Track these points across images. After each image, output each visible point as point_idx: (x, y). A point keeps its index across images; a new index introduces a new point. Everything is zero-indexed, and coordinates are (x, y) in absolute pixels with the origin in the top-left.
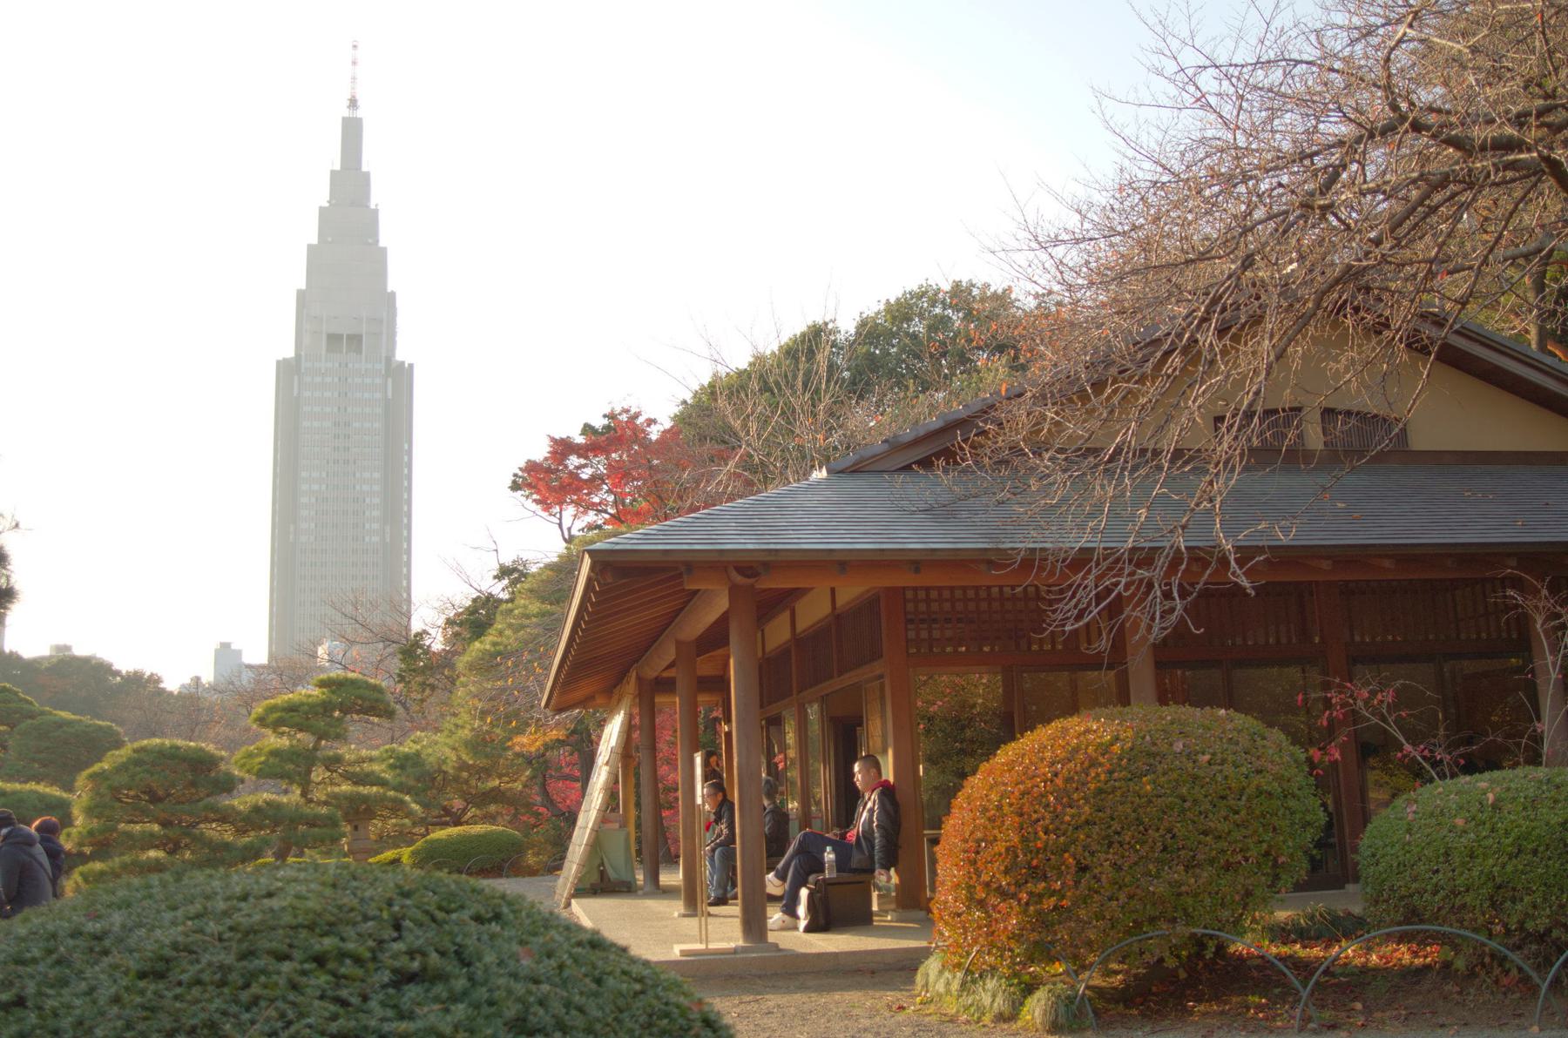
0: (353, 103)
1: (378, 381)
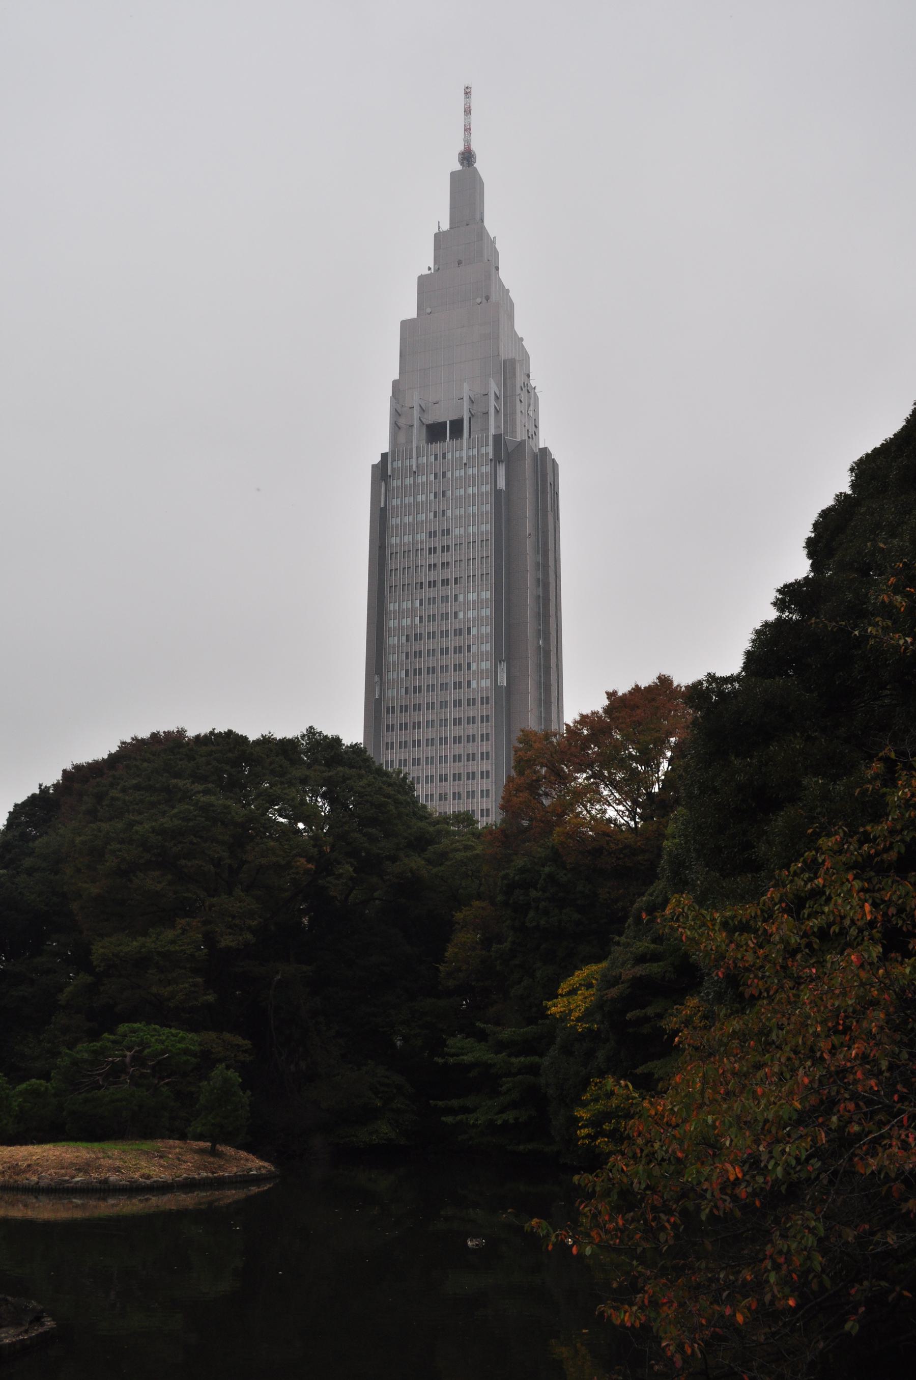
0: (467, 157)
1: (486, 469)
